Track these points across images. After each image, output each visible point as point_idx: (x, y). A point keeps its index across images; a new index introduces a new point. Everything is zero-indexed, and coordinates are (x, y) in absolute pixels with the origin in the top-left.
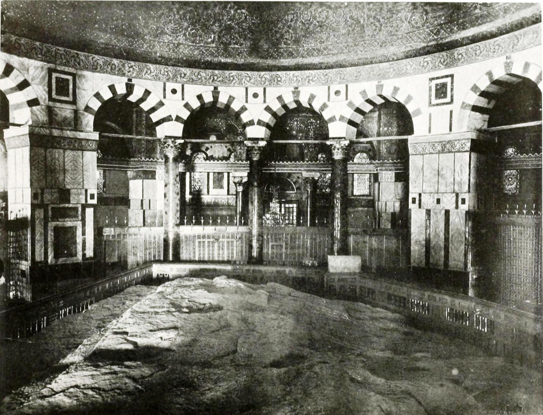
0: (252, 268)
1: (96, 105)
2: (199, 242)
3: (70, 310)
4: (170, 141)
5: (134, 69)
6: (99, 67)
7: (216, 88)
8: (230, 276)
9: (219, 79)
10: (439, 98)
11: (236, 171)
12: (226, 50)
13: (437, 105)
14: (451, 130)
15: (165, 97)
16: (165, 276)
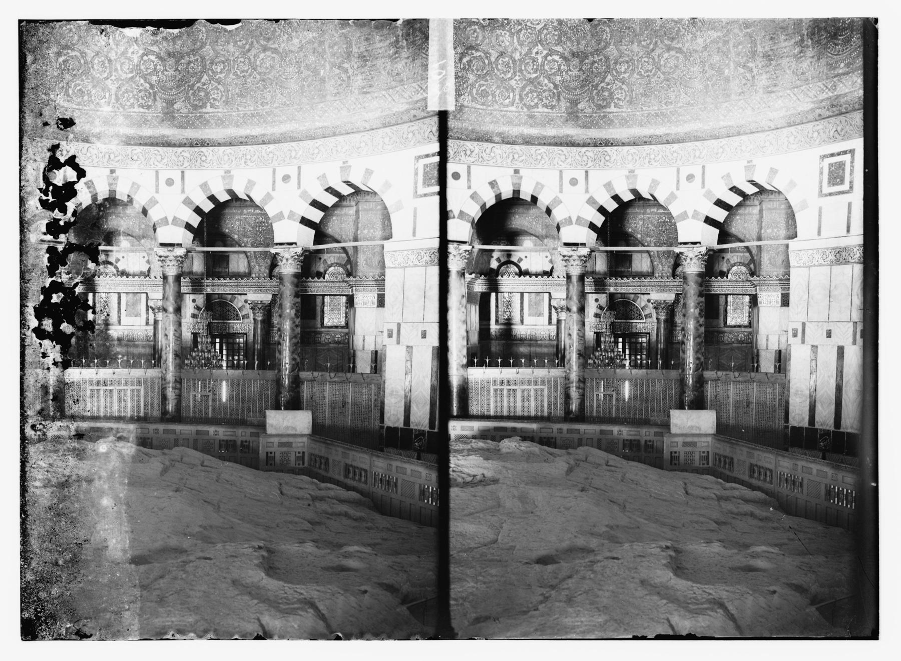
2: (496, 390)
7: (516, 172)
8: (526, 437)
9: (521, 159)
10: (833, 185)
12: (531, 117)
13: (831, 194)
14: (848, 231)
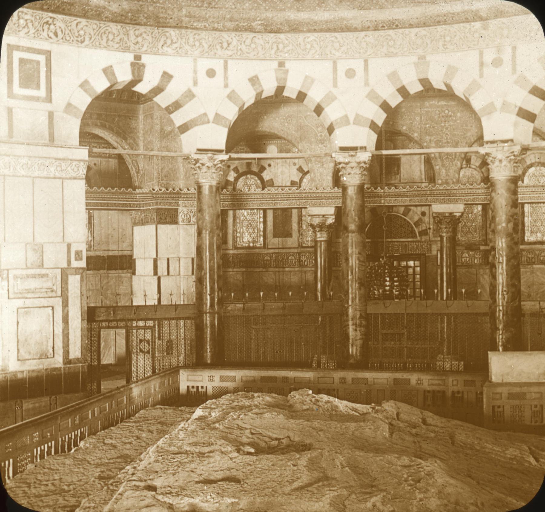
0: (350, 375)
1: (83, 101)
3: (49, 448)
4: (204, 158)
5: (144, 39)
6: (87, 39)
7: (281, 64)
11: (314, 205)
15: (195, 83)
16: (200, 389)
